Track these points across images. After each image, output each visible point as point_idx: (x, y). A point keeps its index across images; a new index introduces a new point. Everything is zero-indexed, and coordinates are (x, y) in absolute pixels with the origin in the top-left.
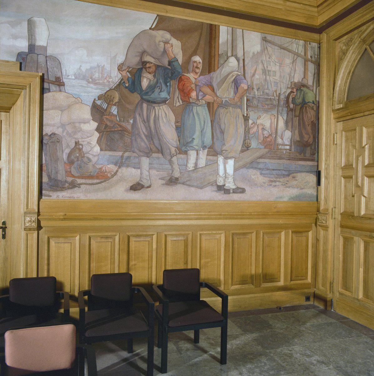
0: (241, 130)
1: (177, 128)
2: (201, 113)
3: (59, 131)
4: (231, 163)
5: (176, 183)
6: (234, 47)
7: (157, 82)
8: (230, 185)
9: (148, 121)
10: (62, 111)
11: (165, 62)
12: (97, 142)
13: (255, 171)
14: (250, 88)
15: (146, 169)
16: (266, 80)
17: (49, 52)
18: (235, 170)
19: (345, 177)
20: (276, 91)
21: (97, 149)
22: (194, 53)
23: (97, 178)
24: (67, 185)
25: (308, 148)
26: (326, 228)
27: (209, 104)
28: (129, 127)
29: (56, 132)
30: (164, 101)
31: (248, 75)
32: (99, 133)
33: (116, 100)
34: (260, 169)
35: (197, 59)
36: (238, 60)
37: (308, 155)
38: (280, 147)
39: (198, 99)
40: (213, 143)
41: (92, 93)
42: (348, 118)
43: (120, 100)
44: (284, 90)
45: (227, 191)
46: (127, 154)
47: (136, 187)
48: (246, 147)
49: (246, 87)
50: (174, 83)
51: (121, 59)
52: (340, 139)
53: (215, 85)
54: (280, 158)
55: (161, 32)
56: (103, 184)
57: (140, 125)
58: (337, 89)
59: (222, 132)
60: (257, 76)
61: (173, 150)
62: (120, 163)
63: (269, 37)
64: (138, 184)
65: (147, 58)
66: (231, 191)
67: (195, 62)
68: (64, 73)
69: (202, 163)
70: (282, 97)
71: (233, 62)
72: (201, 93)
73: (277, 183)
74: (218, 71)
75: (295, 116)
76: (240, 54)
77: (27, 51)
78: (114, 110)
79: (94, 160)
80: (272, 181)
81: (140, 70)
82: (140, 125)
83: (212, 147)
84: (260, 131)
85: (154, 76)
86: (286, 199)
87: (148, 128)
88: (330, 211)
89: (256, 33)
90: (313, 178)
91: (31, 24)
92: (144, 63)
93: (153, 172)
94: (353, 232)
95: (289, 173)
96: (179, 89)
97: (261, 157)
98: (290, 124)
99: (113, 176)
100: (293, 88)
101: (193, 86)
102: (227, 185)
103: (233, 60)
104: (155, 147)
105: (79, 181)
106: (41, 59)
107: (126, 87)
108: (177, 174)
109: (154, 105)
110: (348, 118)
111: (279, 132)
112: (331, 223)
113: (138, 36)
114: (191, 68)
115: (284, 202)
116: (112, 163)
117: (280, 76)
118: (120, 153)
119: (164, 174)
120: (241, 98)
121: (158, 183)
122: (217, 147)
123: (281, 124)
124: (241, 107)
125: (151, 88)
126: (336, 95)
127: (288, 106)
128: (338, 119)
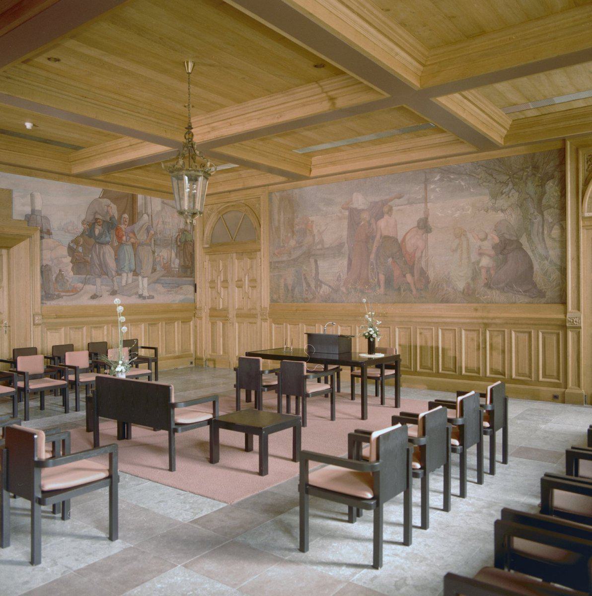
0: (151, 260)
1: (116, 259)
2: (128, 249)
3: (50, 263)
4: (146, 280)
5: (116, 294)
6: (146, 208)
7: (104, 232)
8: (146, 294)
9: (100, 255)
10: (52, 250)
11: (108, 219)
12: (72, 270)
13: (159, 285)
14: (156, 233)
15: (99, 285)
16: (164, 228)
17: (43, 214)
18: (148, 285)
19: (211, 288)
20: (170, 235)
21: (72, 273)
22: (124, 213)
23: (72, 291)
24: (55, 296)
25: (188, 269)
26: (201, 318)
27: (133, 244)
28: (89, 260)
29: (49, 264)
30: (108, 243)
31: (154, 225)
32: (73, 264)
33: (81, 243)
34: (162, 283)
35: (126, 216)
36: (148, 216)
37: (189, 273)
38: (173, 269)
39: (127, 241)
40: (136, 269)
41: (67, 239)
42: (212, 253)
43: (83, 243)
44: (175, 233)
45: (144, 298)
46: (88, 276)
47: (94, 297)
48: (154, 270)
49: (153, 233)
50: (113, 232)
51: (83, 217)
52: (207, 264)
53: (136, 231)
54: (173, 277)
55: (105, 200)
56: (75, 295)
57: (95, 257)
58: (205, 235)
59: (141, 262)
60: (159, 226)
61: (114, 273)
62: (85, 282)
63: (166, 201)
64: (95, 295)
65: (98, 216)
66: (146, 298)
67: (125, 218)
68: (52, 227)
69: (130, 281)
70: (174, 238)
71: (145, 217)
72: (128, 238)
73: (172, 292)
74: (137, 223)
75: (181, 250)
76: (149, 211)
77: (30, 213)
78: (80, 249)
79: (70, 280)
80: (169, 291)
81: (94, 223)
82: (95, 257)
83: (135, 271)
84: (162, 259)
85: (102, 227)
86: (177, 302)
87: (99, 259)
88: (203, 308)
89: (157, 199)
90: (192, 288)
91: (32, 196)
92: (96, 219)
93: (103, 287)
94: (217, 319)
95: (179, 286)
96: (116, 235)
97: (163, 276)
98: (178, 255)
99: (81, 290)
100: (179, 233)
101: (124, 233)
102: (144, 294)
103: (145, 216)
104: (104, 271)
105: (62, 294)
106: (39, 218)
107: (87, 235)
108: (116, 288)
109: (103, 246)
110: (212, 253)
111: (172, 261)
112: (204, 315)
113: (92, 203)
114: (122, 222)
115: (176, 304)
116: (80, 282)
117: (172, 225)
118: (84, 276)
119: (108, 288)
120: (151, 239)
121: (106, 294)
122: (138, 272)
123: (173, 255)
124: (150, 245)
125: (101, 235)
126: (205, 239)
127: (177, 244)
128: (207, 253)
